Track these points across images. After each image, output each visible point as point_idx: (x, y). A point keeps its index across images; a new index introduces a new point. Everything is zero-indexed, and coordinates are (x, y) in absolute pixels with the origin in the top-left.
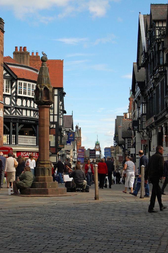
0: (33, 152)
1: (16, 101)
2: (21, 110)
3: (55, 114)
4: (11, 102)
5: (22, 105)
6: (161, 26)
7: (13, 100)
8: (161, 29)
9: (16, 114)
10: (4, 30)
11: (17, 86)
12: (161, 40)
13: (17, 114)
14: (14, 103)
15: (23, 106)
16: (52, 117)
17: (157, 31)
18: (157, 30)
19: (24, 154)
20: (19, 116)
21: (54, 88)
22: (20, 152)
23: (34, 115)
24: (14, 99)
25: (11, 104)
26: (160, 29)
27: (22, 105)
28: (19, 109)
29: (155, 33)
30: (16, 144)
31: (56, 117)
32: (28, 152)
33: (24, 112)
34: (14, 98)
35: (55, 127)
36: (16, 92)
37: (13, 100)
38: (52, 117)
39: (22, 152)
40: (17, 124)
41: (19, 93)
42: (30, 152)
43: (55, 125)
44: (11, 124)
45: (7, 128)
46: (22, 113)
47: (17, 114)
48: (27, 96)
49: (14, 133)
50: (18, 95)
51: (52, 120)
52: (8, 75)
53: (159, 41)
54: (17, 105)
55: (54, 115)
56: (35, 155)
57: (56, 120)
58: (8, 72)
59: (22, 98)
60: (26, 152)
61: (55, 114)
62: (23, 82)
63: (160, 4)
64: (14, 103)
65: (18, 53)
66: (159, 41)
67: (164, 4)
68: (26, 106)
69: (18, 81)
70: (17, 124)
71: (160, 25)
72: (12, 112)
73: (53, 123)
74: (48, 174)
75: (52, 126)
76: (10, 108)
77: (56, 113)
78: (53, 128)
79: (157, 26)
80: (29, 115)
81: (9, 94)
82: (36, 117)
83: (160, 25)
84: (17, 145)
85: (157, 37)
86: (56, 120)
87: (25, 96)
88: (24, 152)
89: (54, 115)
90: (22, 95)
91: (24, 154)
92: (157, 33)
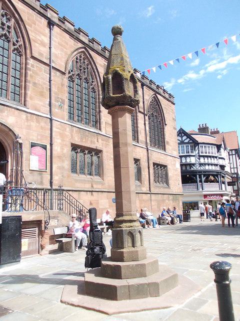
1: (199, 159)
21: (232, 150)
38: (232, 170)
40: (202, 176)
44: (198, 176)
50: (201, 154)
52: (191, 141)
55: (234, 168)
57: (236, 172)
58: (191, 140)
59: (203, 156)
62: (203, 145)
69: (200, 145)
70: (202, 176)
74: (130, 244)
76: (195, 164)
87: (206, 155)
89: (234, 168)
90: (204, 154)
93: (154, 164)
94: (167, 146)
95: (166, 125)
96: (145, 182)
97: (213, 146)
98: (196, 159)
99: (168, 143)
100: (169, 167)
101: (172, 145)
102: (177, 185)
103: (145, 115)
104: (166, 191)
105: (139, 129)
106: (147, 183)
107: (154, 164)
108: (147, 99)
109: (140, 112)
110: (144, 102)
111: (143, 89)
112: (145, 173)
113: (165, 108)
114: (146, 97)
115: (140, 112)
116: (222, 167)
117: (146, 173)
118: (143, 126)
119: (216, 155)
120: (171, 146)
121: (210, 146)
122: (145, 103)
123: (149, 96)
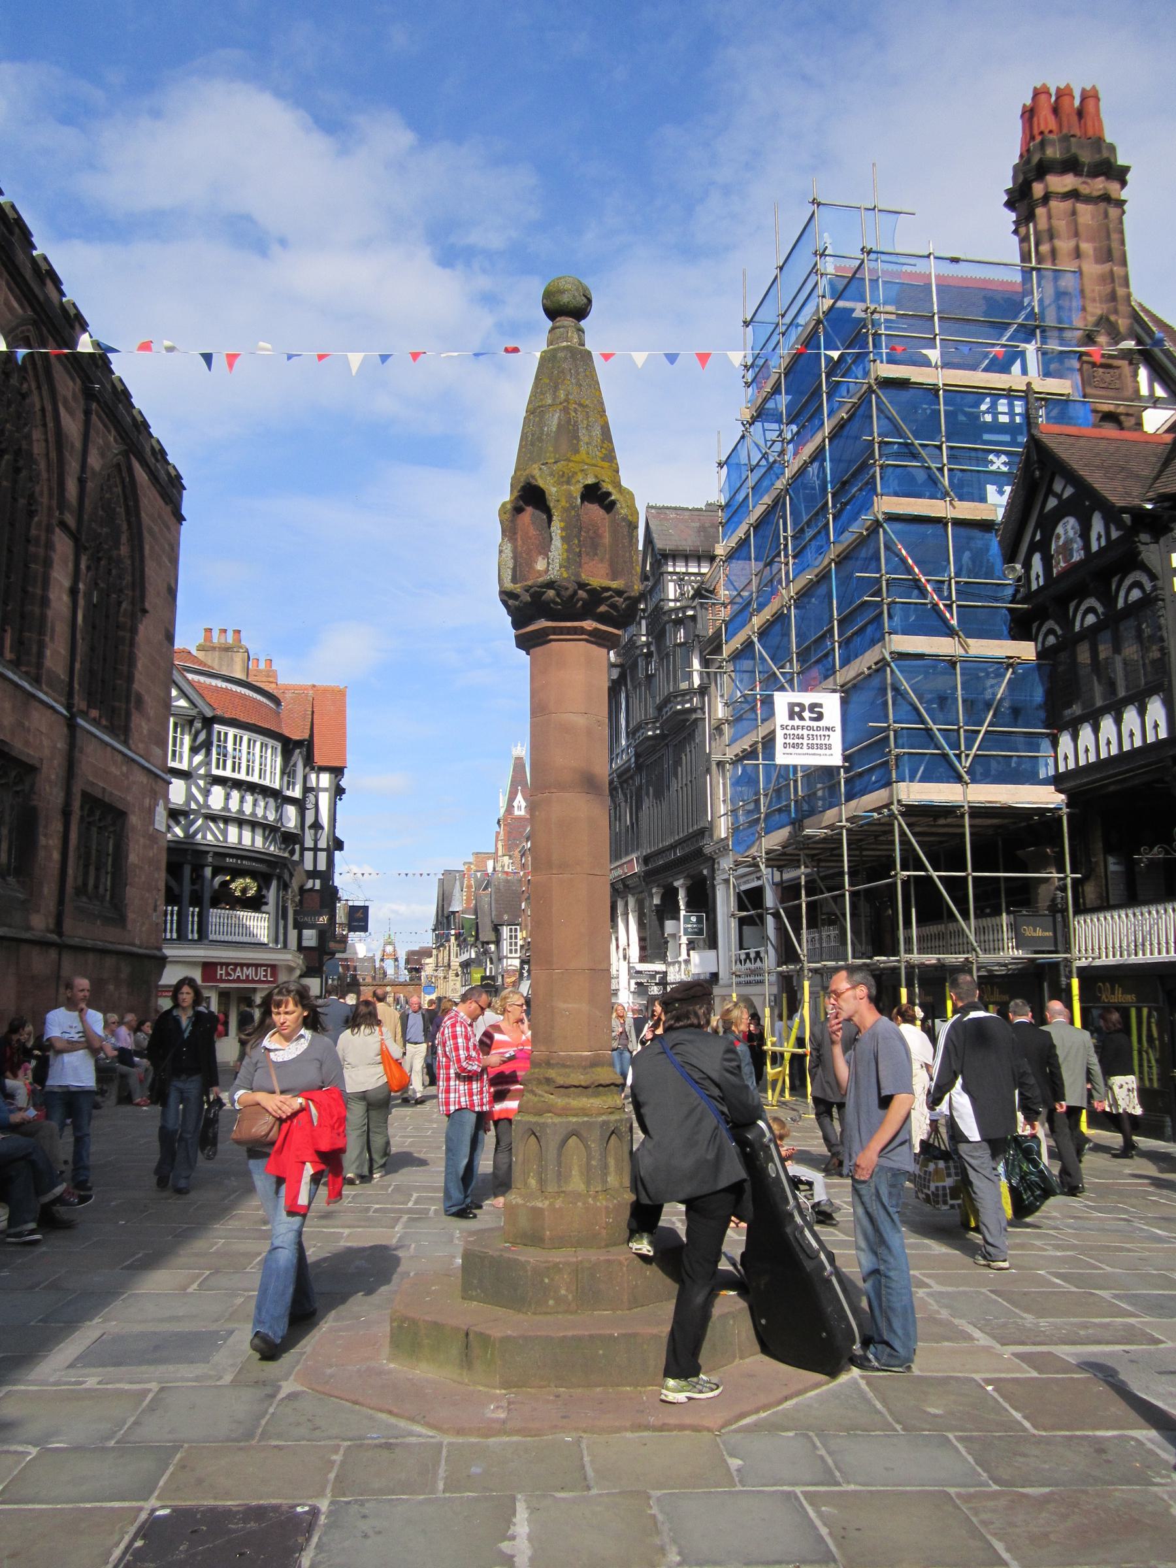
0: (257, 966)
1: (206, 793)
2: (222, 826)
3: (311, 853)
4: (190, 797)
5: (226, 808)
6: (684, 570)
7: (194, 790)
8: (682, 580)
9: (204, 837)
10: (184, 512)
11: (211, 744)
12: (684, 613)
13: (209, 837)
14: (201, 799)
15: (229, 810)
16: (309, 855)
17: (671, 586)
18: (672, 581)
19: (228, 974)
20: (215, 843)
22: (216, 964)
23: (264, 844)
24: (198, 787)
25: (187, 802)
26: (681, 579)
27: (226, 808)
28: (213, 818)
29: (664, 590)
30: (200, 938)
31: (322, 856)
32: (242, 965)
33: (233, 831)
34: (201, 783)
35: (318, 887)
36: (207, 763)
37: (194, 790)
39: (222, 964)
41: (218, 767)
42: (248, 965)
43: (318, 882)
44: (187, 870)
45: (173, 884)
46: (225, 833)
47: (209, 837)
48: (242, 776)
49: (196, 900)
50: (215, 772)
51: (308, 866)
53: (677, 615)
54: (209, 807)
55: (315, 850)
56: (265, 976)
60: (236, 965)
61: (311, 853)
62: (232, 732)
63: (675, 509)
64: (201, 799)
65: (214, 649)
66: (677, 615)
67: (687, 509)
68: (241, 811)
69: (217, 727)
71: (680, 568)
72: (192, 830)
73: (314, 874)
75: (309, 884)
76: (185, 814)
77: (323, 844)
78: (311, 890)
79: (671, 569)
80: (249, 843)
81: (184, 766)
82: (272, 848)
83: (680, 568)
84: (206, 942)
85: (672, 604)
86: (322, 866)
87: (236, 776)
88: (228, 964)
89: (315, 850)
91: (228, 974)
92: (672, 590)
93: (85, 795)
94: (136, 720)
95: (144, 611)
96: (46, 891)
97: (271, 742)
98: (188, 790)
99: (139, 701)
100: (134, 819)
101: (152, 713)
102: (150, 911)
103: (79, 549)
104: (107, 936)
105: (50, 613)
106: (49, 890)
107: (85, 795)
108: (93, 472)
109: (63, 525)
110: (82, 482)
111: (87, 413)
112: (49, 841)
113: (150, 531)
114: (95, 461)
115: (63, 525)
116: (290, 839)
117: (51, 842)
118: (65, 598)
119: (277, 786)
120: (149, 720)
121: (259, 739)
122: (90, 485)
123: (103, 455)
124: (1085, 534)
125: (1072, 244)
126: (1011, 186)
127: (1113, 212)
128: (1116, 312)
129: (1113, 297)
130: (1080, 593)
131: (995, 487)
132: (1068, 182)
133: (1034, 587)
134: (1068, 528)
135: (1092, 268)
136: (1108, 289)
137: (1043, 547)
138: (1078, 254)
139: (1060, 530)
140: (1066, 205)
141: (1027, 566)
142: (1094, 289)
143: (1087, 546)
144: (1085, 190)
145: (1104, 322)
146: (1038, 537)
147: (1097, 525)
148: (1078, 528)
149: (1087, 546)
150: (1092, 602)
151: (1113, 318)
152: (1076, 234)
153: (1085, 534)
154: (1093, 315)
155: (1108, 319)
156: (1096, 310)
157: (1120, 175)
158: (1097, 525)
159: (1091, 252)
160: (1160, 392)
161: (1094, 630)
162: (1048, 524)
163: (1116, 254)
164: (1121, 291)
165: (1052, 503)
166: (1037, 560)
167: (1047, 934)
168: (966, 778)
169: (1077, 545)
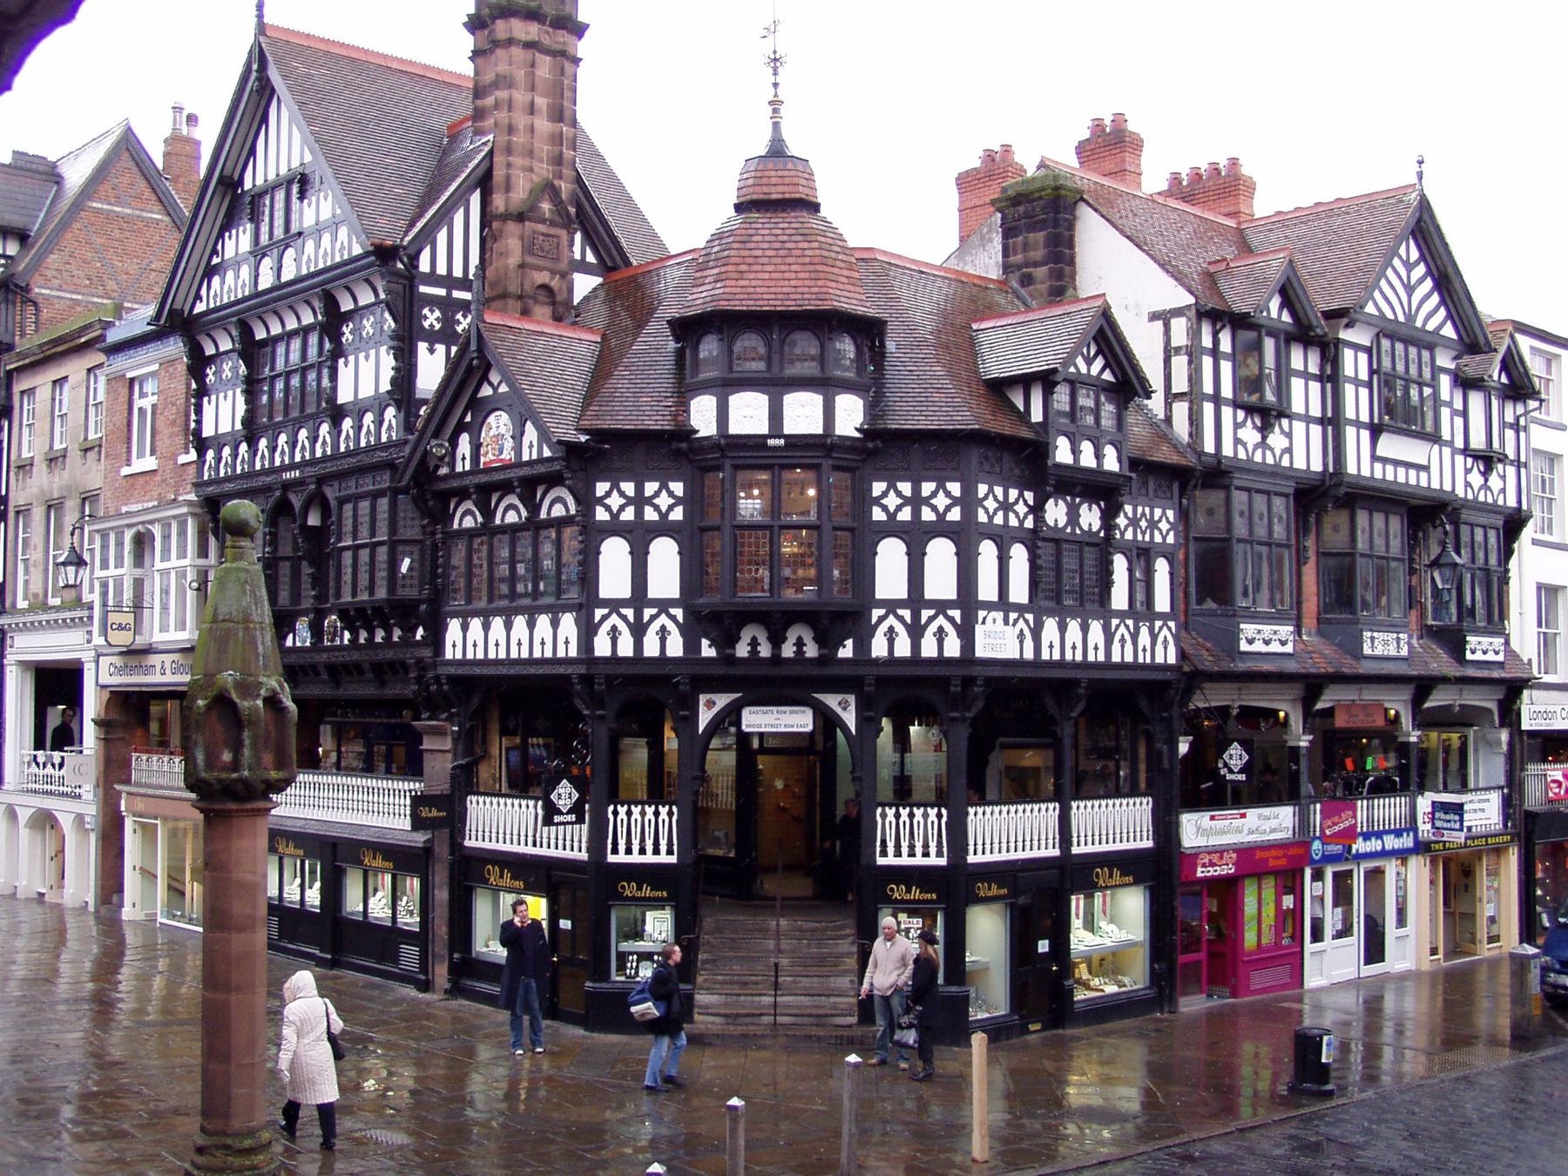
124: (518, 436)
125: (528, 97)
126: (472, 11)
127: (568, 65)
128: (560, 177)
129: (558, 160)
130: (505, 488)
131: (426, 345)
132: (530, 31)
133: (459, 469)
134: (499, 423)
135: (543, 125)
136: (557, 149)
137: (475, 430)
138: (532, 109)
139: (491, 419)
140: (529, 54)
141: (454, 443)
142: (544, 149)
143: (518, 449)
144: (546, 41)
145: (550, 189)
146: (468, 419)
147: (531, 434)
148: (510, 423)
149: (518, 449)
150: (512, 499)
151: (556, 182)
152: (533, 89)
153: (518, 436)
154: (538, 176)
155: (553, 185)
156: (544, 170)
157: (579, 30)
158: (531, 434)
159: (545, 108)
160: (591, 258)
161: (514, 529)
162: (482, 409)
163: (567, 114)
164: (568, 153)
165: (486, 391)
166: (464, 441)
167: (441, 814)
168: (386, 667)
169: (509, 444)
